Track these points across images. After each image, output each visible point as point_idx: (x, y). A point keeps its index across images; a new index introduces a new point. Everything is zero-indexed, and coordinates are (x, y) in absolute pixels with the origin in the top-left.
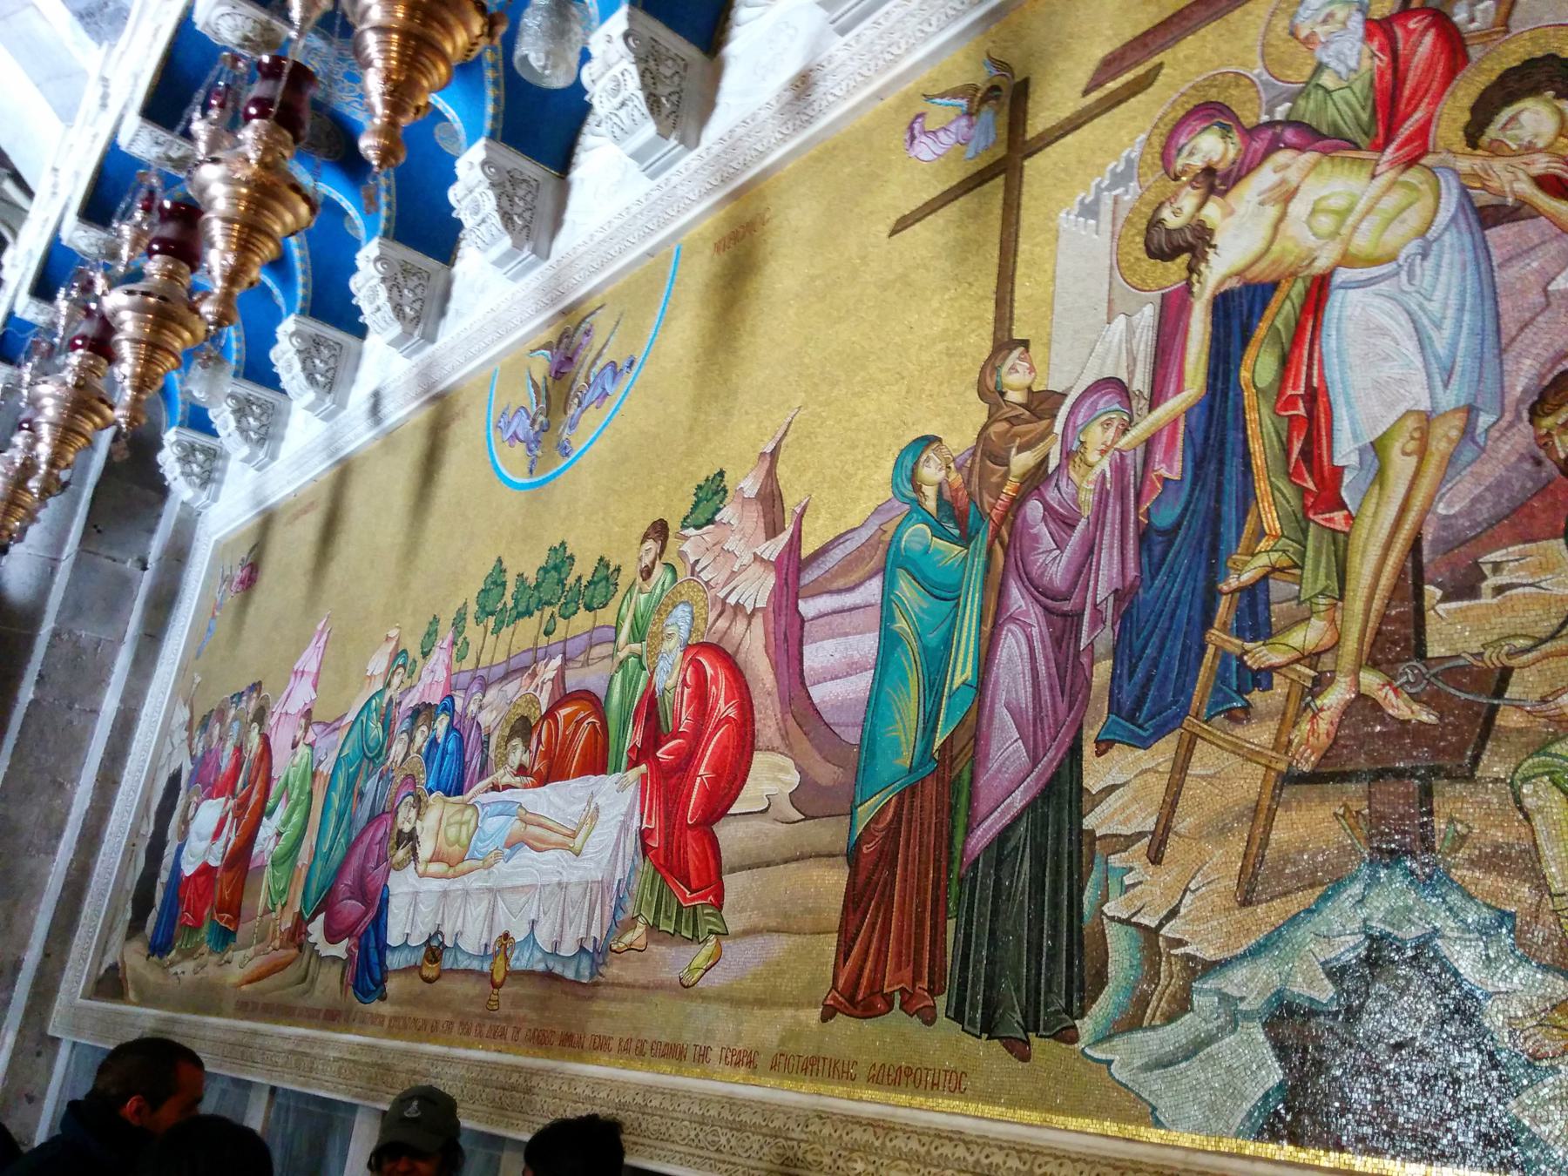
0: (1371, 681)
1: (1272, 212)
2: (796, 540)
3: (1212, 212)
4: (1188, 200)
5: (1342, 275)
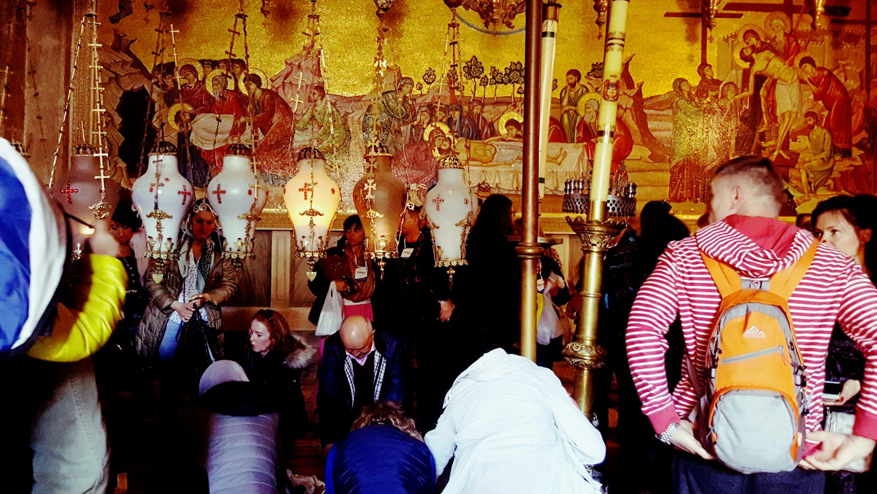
0: (781, 152)
1: (766, 62)
2: (639, 93)
3: (754, 55)
4: (750, 51)
5: (779, 81)
